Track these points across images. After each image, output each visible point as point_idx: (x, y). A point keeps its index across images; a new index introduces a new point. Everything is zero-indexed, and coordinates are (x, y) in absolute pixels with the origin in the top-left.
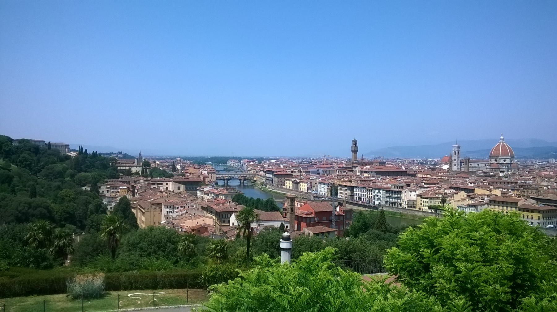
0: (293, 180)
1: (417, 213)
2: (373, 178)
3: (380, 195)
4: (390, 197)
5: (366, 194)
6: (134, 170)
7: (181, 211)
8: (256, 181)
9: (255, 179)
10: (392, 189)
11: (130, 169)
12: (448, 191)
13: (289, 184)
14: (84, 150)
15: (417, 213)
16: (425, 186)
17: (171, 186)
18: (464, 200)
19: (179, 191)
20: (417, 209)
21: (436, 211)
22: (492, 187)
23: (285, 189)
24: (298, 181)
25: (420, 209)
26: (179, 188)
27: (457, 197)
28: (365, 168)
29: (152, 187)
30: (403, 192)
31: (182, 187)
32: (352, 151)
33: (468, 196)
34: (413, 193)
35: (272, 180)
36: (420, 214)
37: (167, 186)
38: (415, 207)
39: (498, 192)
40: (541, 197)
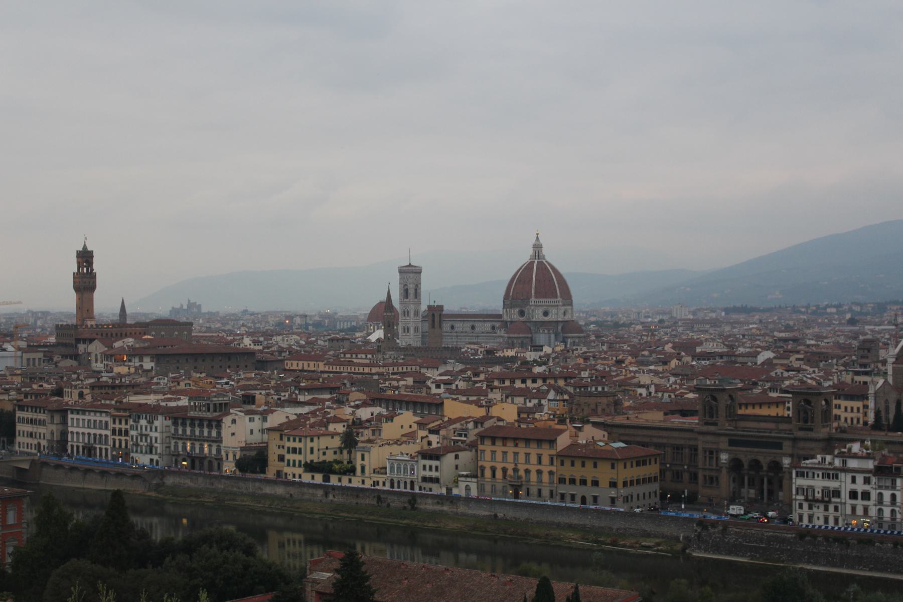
1: (268, 490)
2: (143, 379)
3: (154, 434)
4: (183, 438)
5: (109, 433)
10: (192, 414)
12: (364, 414)
15: (268, 490)
16: (301, 398)
18: (411, 436)
20: (270, 474)
21: (326, 479)
22: (491, 396)
25: (279, 473)
27: (390, 430)
28: (117, 345)
30: (227, 420)
32: (77, 289)
33: (421, 425)
34: (257, 424)
36: (280, 490)
38: (264, 473)
39: (507, 412)
40: (620, 420)
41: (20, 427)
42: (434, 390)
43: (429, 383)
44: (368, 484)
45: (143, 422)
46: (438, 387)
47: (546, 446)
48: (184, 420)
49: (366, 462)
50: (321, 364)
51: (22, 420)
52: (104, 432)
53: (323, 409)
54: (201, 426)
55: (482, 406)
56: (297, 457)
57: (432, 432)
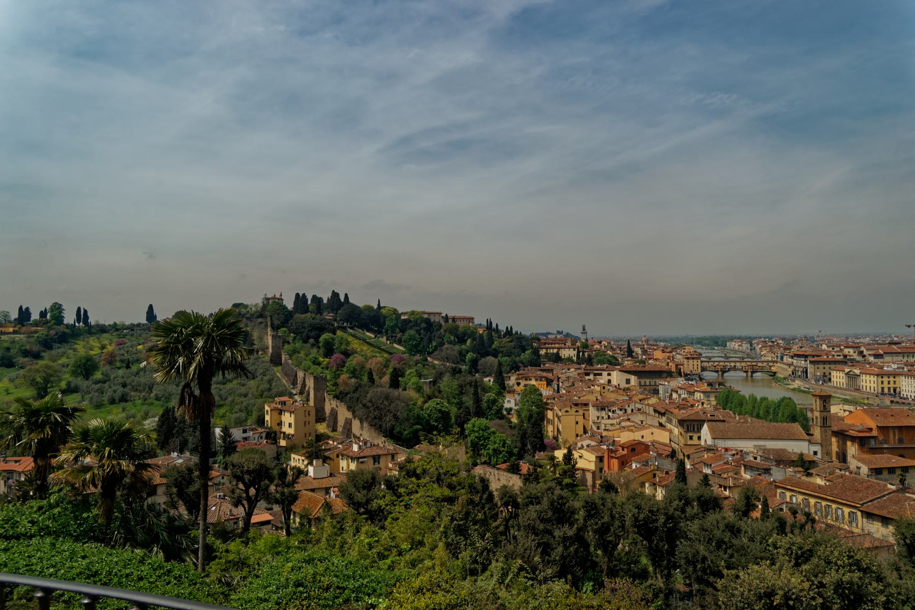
0: (847, 370)
6: (566, 353)
8: (775, 373)
9: (774, 369)
11: (558, 353)
13: (838, 377)
14: (494, 326)
17: (617, 378)
19: (627, 386)
23: (830, 387)
24: (857, 372)
26: (628, 381)
29: (587, 378)
31: (633, 379)
35: (806, 372)
37: (609, 377)
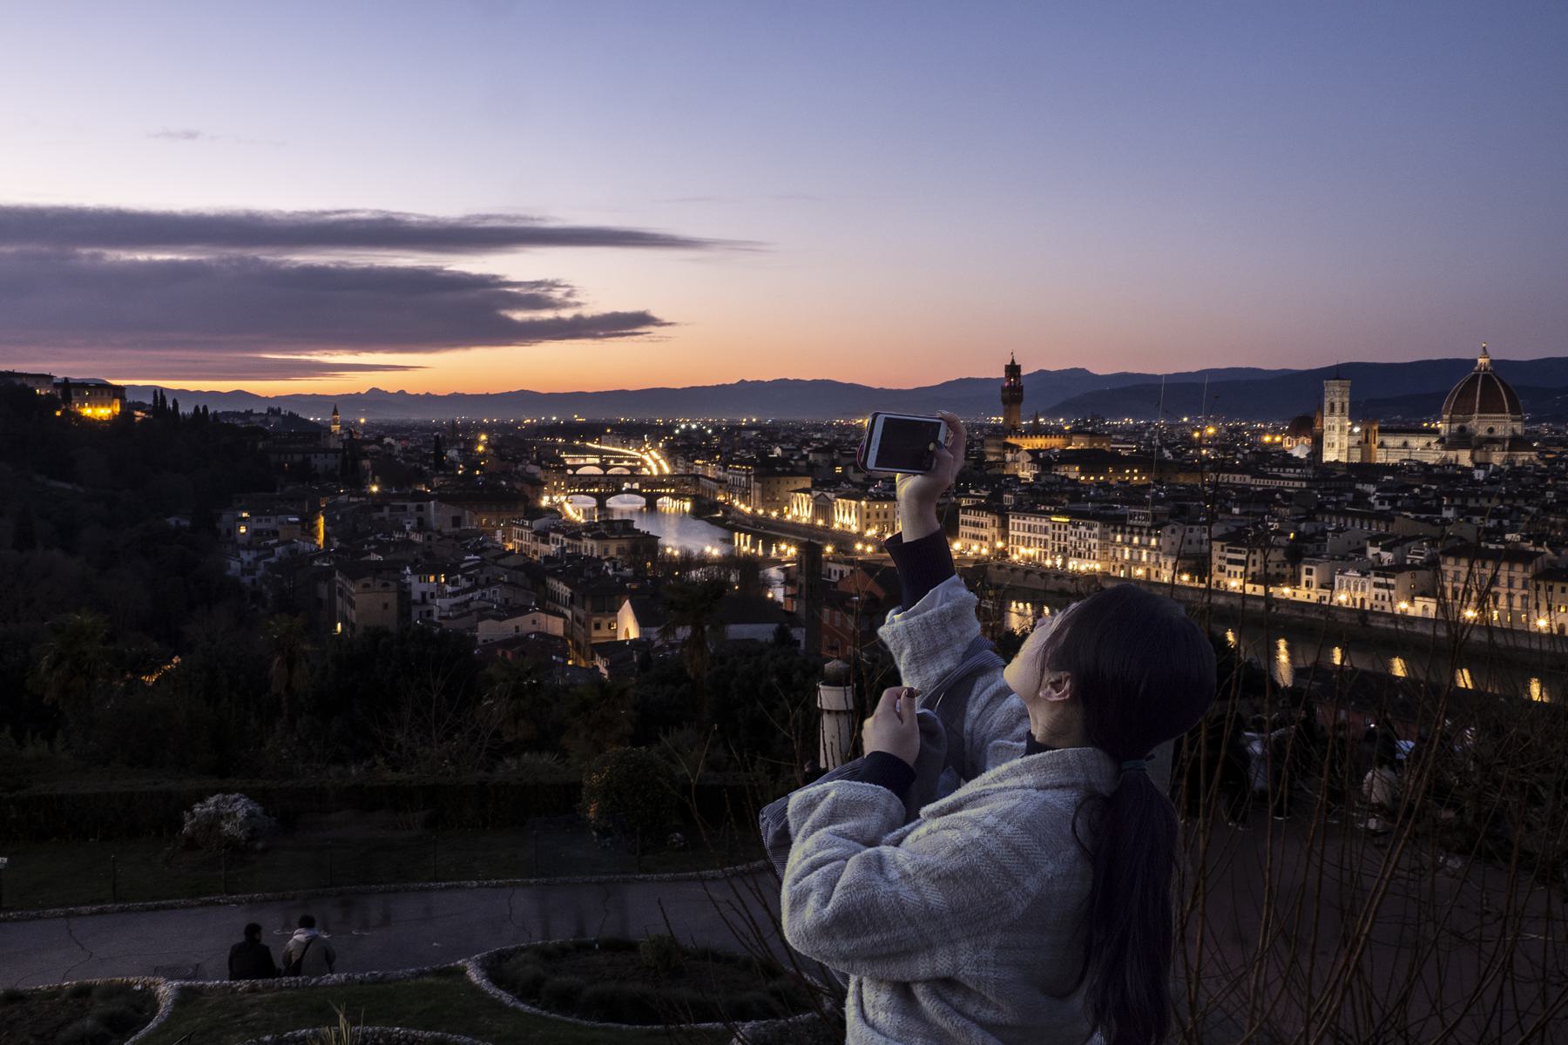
7: (465, 591)
39: (1469, 532)
41: (963, 529)
42: (1378, 507)
43: (1372, 499)
44: (1314, 598)
45: (1083, 529)
46: (1382, 503)
47: (1519, 568)
48: (1124, 525)
49: (1314, 578)
50: (1248, 478)
51: (966, 523)
52: (1044, 537)
53: (1263, 521)
54: (1140, 534)
55: (1436, 525)
56: (1241, 569)
57: (1383, 549)
